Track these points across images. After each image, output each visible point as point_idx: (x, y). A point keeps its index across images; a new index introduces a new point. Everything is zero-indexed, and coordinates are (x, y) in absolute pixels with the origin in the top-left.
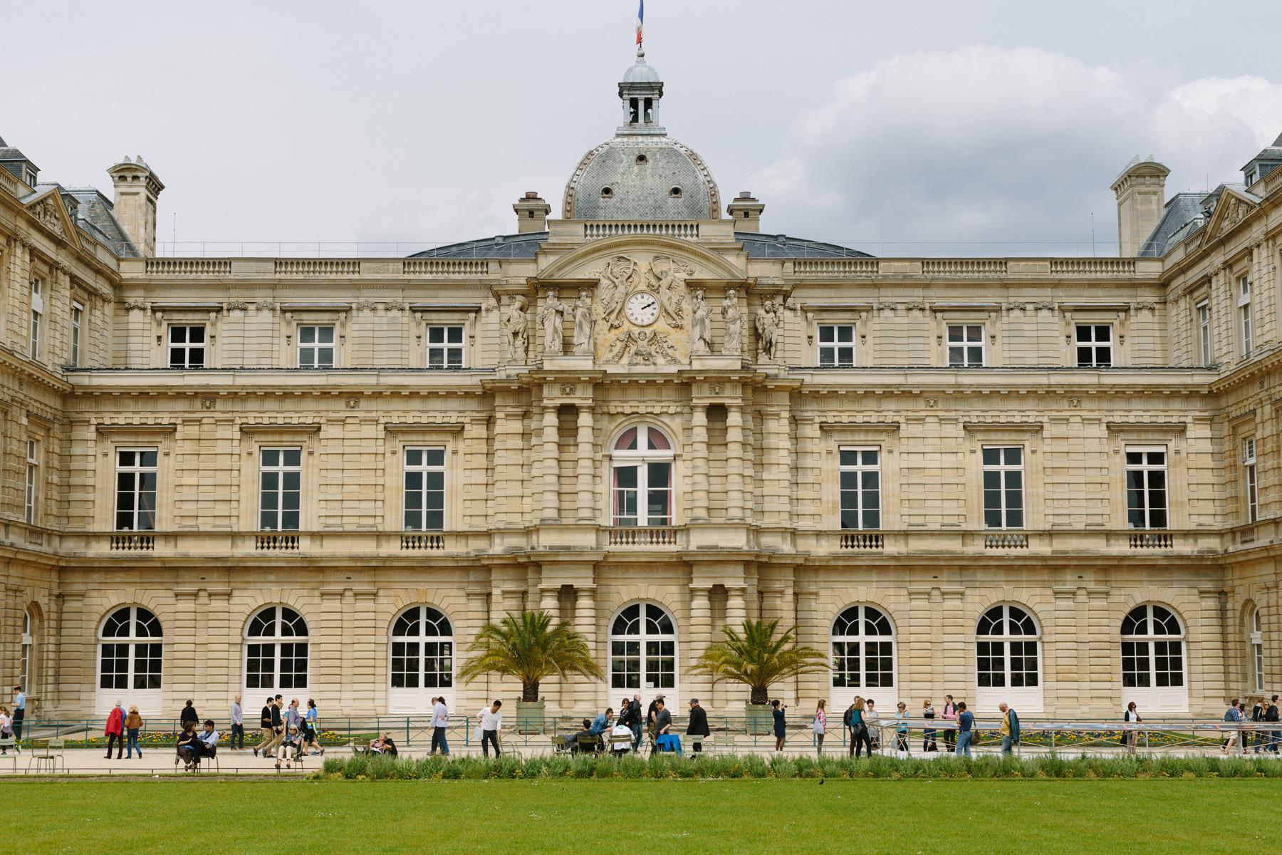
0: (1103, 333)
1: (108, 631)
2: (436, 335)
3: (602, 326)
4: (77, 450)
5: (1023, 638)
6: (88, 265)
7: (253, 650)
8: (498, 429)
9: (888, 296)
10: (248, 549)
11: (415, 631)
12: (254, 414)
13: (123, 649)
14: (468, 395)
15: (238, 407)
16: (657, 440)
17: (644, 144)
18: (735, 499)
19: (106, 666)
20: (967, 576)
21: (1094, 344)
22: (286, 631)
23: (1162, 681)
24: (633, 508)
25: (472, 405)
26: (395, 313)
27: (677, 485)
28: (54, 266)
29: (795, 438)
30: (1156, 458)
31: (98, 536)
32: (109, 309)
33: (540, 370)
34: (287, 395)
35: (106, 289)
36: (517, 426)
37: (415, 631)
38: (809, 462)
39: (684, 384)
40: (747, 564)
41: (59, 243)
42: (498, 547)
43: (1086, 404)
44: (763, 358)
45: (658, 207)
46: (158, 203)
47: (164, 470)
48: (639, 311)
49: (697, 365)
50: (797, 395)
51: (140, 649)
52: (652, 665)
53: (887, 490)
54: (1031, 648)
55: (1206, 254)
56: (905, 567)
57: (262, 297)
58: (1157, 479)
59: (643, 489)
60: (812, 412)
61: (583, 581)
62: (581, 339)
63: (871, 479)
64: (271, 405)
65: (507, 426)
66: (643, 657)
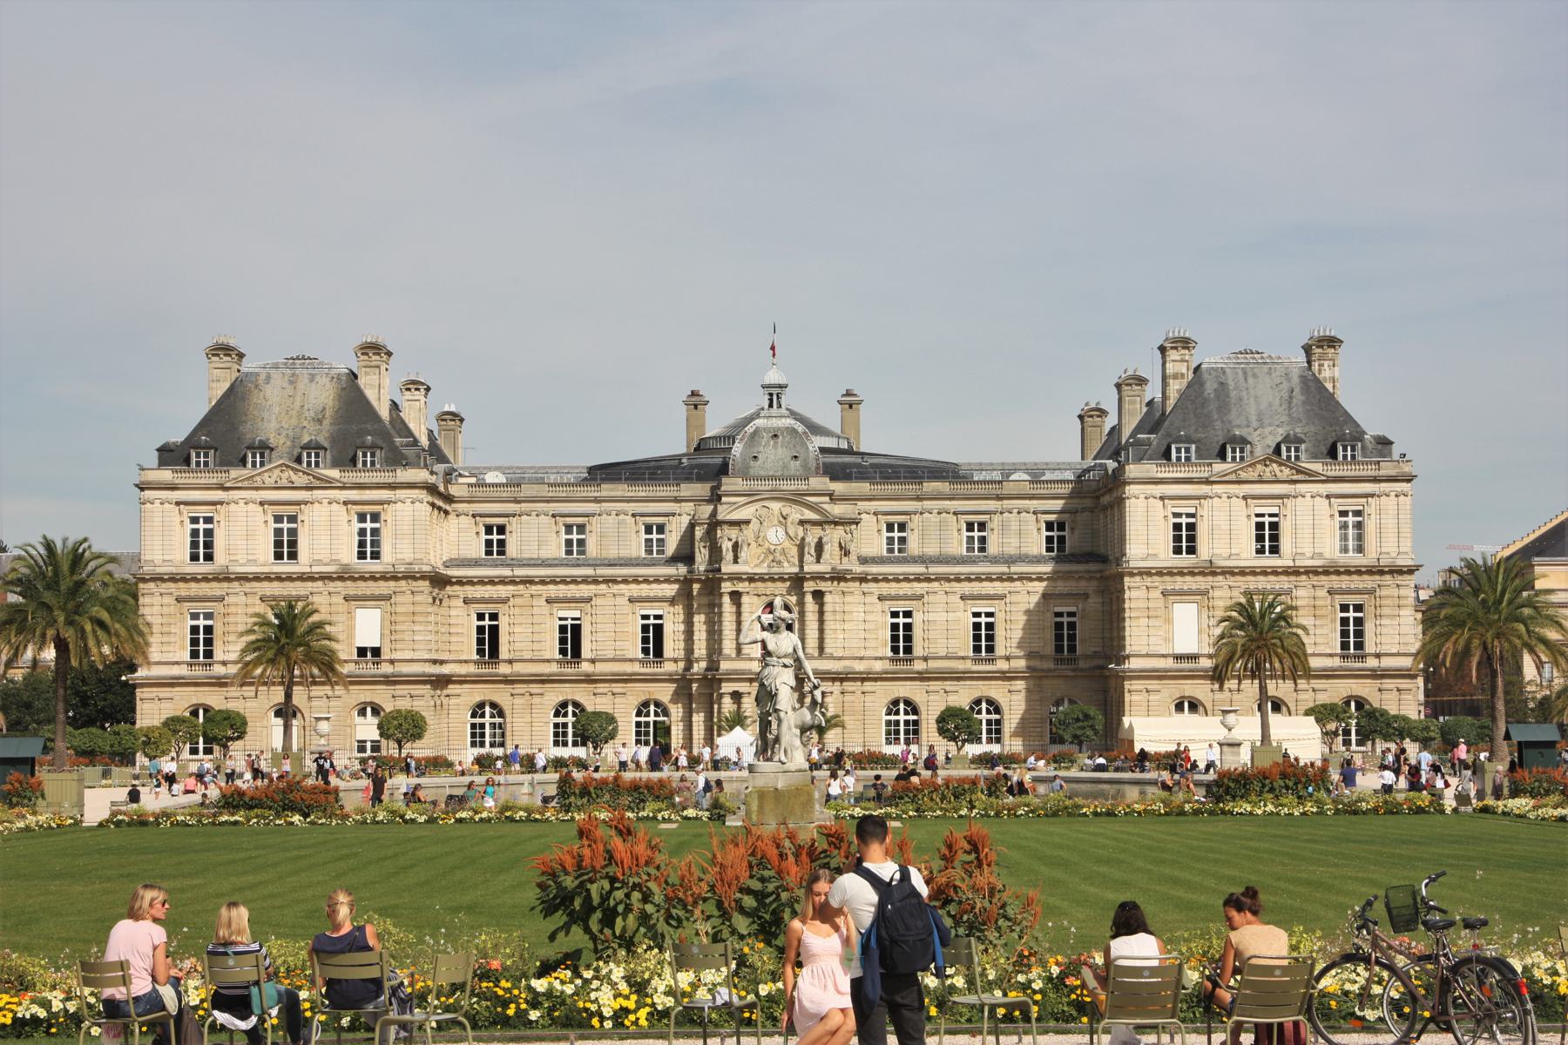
1: (474, 715)
2: (649, 530)
3: (754, 545)
7: (556, 726)
9: (927, 504)
13: (482, 726)
14: (677, 581)
18: (828, 643)
19: (473, 735)
26: (622, 517)
33: (719, 570)
36: (705, 600)
37: (648, 715)
38: (869, 617)
44: (845, 560)
45: (785, 467)
47: (503, 622)
48: (775, 535)
53: (917, 633)
58: (1072, 626)
62: (743, 555)
63: (908, 627)
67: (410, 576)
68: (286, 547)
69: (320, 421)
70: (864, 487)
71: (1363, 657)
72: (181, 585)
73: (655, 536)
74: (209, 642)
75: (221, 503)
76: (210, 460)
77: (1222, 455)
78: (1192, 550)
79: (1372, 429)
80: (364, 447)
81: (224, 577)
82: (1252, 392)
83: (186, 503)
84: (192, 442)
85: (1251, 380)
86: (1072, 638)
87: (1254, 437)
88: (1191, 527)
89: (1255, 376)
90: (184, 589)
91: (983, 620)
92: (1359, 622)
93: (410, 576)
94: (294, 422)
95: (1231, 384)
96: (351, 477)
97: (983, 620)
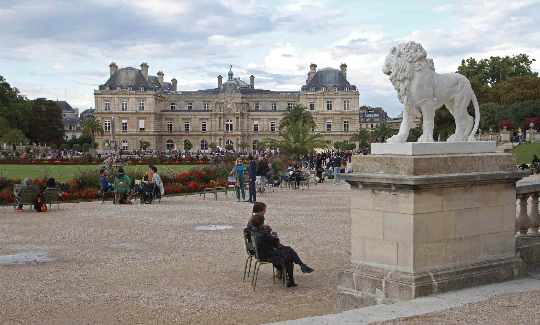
2: (205, 105)
9: (264, 99)
10: (184, 133)
12: (183, 117)
16: (231, 121)
17: (231, 82)
27: (233, 127)
34: (187, 115)
35: (163, 99)
39: (234, 115)
42: (213, 133)
47: (173, 124)
48: (229, 106)
50: (248, 115)
56: (261, 135)
57: (183, 99)
59: (229, 127)
60: (251, 117)
61: (222, 138)
62: (222, 110)
67: (150, 114)
68: (124, 107)
70: (251, 95)
71: (348, 132)
75: (111, 98)
77: (320, 90)
79: (352, 83)
80: (141, 87)
81: (112, 113)
83: (104, 98)
84: (105, 85)
87: (328, 86)
88: (314, 105)
92: (348, 125)
93: (150, 114)
96: (138, 92)
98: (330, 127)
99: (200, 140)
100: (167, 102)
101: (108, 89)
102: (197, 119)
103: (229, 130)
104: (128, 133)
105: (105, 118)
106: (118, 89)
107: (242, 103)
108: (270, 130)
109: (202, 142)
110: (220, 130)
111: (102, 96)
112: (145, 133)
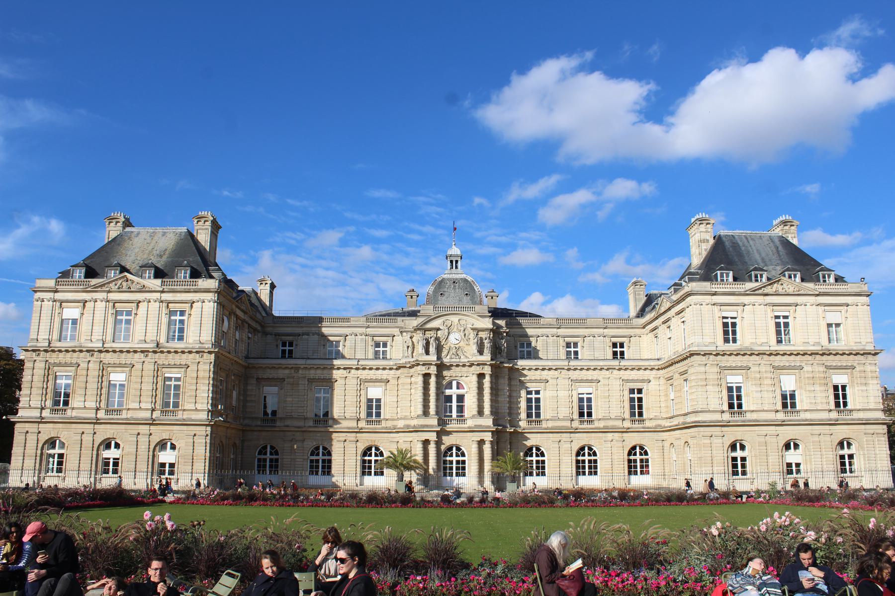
0: (622, 345)
1: (260, 453)
2: (377, 345)
4: (249, 388)
5: (593, 458)
6: (254, 320)
8: (400, 381)
11: (370, 455)
12: (312, 374)
13: (265, 460)
14: (391, 369)
15: (307, 372)
16: (459, 386)
19: (259, 466)
20: (572, 435)
21: (618, 349)
22: (324, 455)
23: (642, 473)
24: (451, 412)
25: (393, 372)
28: (243, 321)
29: (510, 385)
30: (640, 391)
31: (256, 418)
32: (260, 335)
35: (259, 328)
36: (408, 380)
37: (370, 455)
40: (492, 432)
41: (245, 313)
42: (401, 424)
43: (615, 372)
44: (499, 356)
46: (274, 292)
48: (454, 338)
49: (474, 359)
51: (271, 460)
52: (457, 468)
54: (595, 461)
55: (657, 318)
58: (640, 400)
59: (454, 404)
62: (432, 349)
63: (538, 400)
64: (319, 372)
65: (405, 380)
66: (454, 465)
69: (161, 256)
72: (54, 355)
73: (381, 349)
74: (67, 395)
76: (83, 275)
77: (751, 281)
78: (734, 341)
82: (754, 248)
83: (61, 302)
85: (751, 242)
86: (640, 407)
88: (734, 325)
89: (752, 239)
90: (53, 358)
91: (585, 396)
92: (844, 388)
94: (145, 256)
95: (741, 244)
97: (585, 396)
98: (793, 396)
99: (362, 447)
100: (270, 338)
101: (79, 273)
102: (355, 381)
103: (454, 414)
104: (124, 415)
105: (60, 365)
106: (112, 274)
107: (496, 331)
108: (576, 416)
109: (367, 452)
110: (426, 413)
111: (58, 296)
112: (180, 415)
